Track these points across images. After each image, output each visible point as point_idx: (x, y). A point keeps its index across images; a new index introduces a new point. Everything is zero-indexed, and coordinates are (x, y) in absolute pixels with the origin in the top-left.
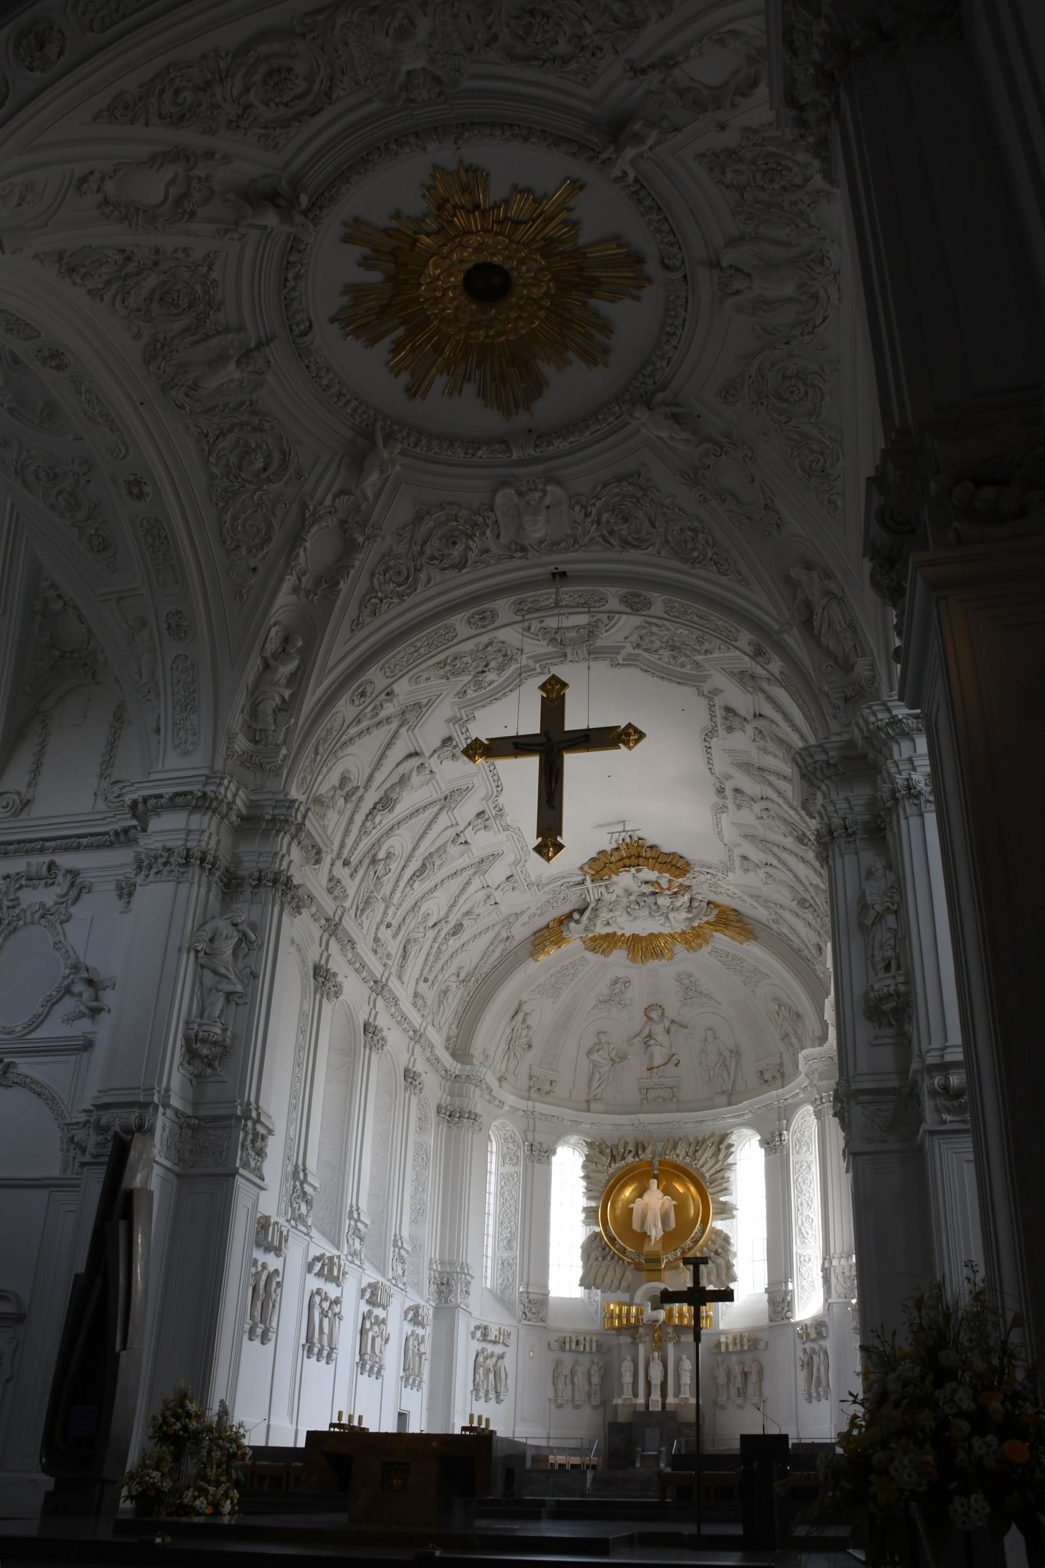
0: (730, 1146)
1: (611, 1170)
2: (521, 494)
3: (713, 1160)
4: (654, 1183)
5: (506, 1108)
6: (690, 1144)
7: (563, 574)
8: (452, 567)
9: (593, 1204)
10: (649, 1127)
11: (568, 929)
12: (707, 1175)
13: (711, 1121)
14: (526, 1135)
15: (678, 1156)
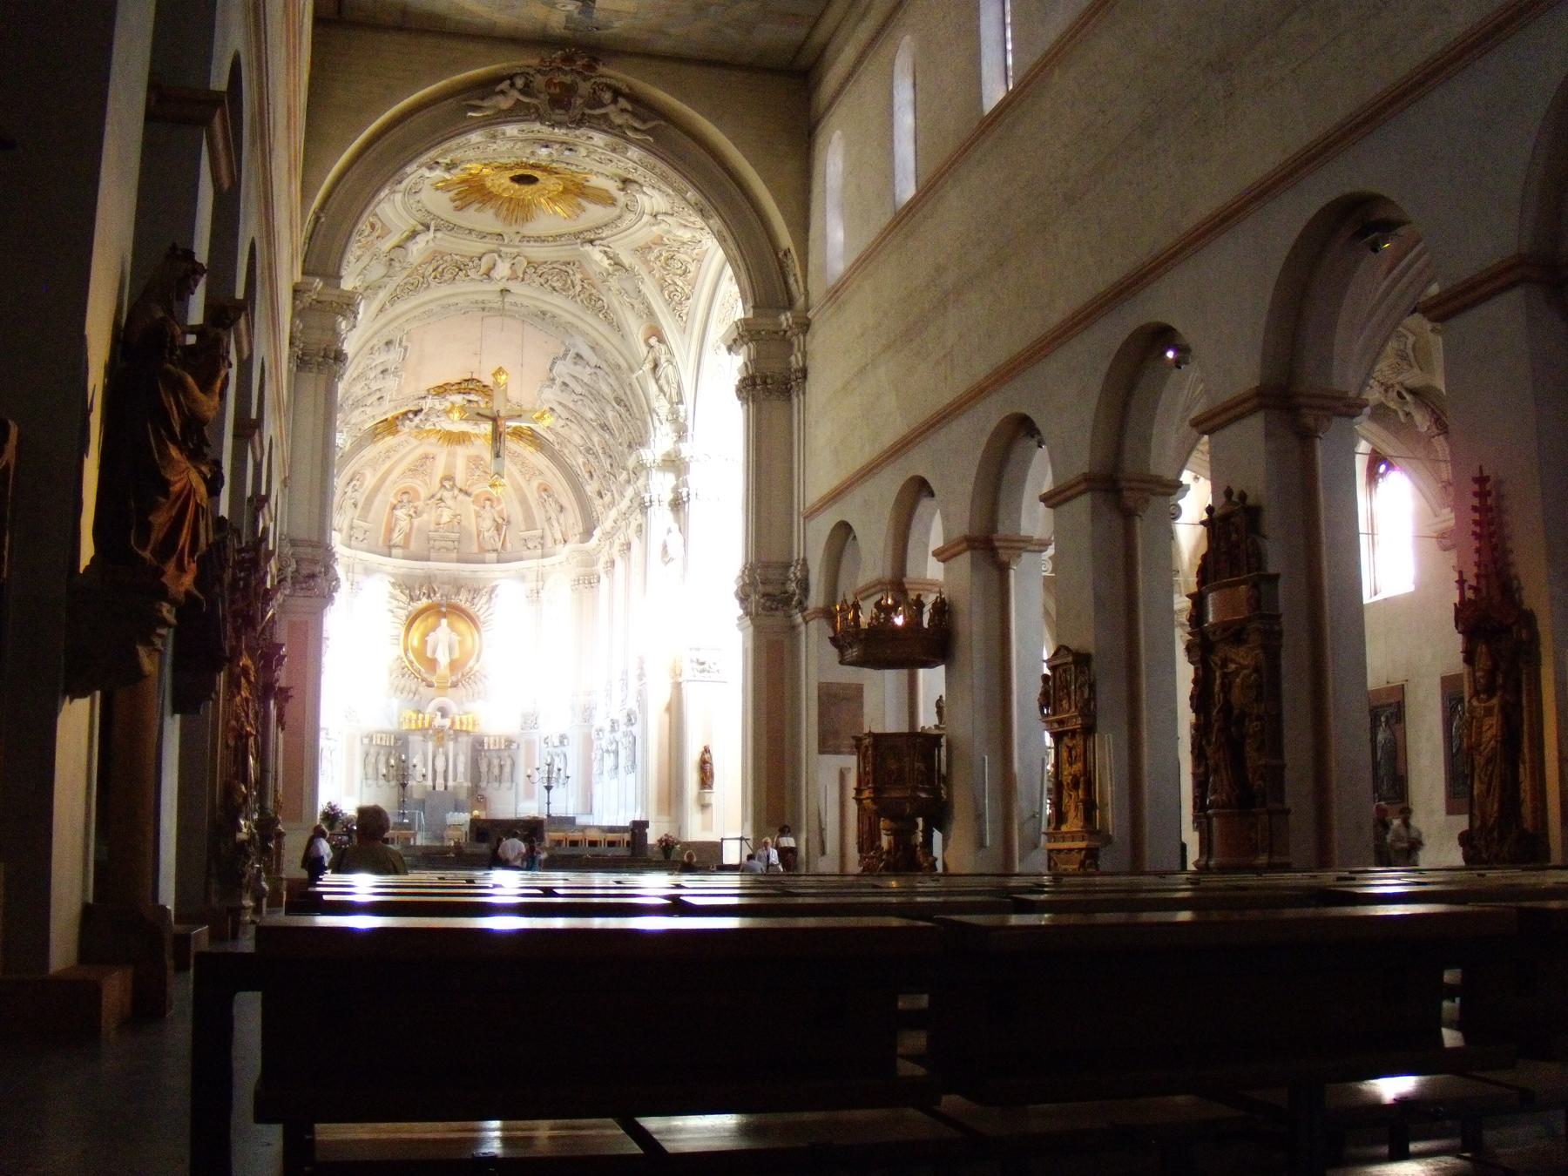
0: (497, 596)
1: (410, 608)
3: (486, 607)
6: (469, 591)
9: (395, 632)
10: (436, 572)
11: (403, 425)
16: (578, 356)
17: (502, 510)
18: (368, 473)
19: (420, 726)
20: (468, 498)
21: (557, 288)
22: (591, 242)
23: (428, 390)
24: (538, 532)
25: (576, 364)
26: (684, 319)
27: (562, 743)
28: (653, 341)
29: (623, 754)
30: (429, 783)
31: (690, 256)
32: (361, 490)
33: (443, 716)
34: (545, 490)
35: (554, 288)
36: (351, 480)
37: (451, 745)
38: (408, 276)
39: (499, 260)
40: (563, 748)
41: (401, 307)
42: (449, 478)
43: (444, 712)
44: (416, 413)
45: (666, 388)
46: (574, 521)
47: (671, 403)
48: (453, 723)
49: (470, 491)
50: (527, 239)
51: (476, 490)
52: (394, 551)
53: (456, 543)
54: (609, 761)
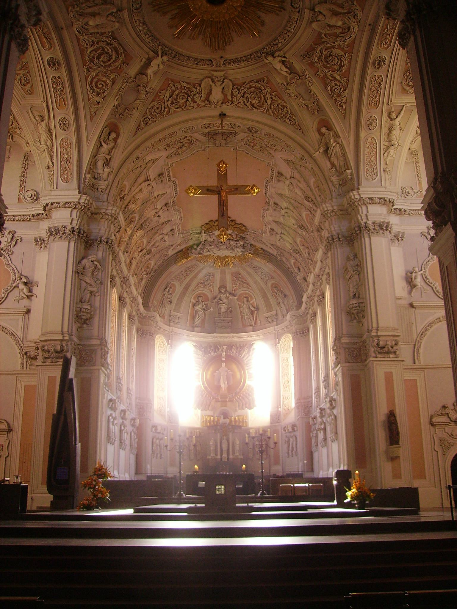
0: (254, 349)
2: (213, 82)
4: (223, 365)
5: (162, 330)
7: (225, 115)
8: (180, 107)
10: (219, 339)
12: (245, 361)
13: (244, 337)
14: (169, 342)
15: (233, 353)
16: (279, 173)
17: (254, 303)
18: (177, 284)
19: (212, 423)
20: (234, 297)
21: (255, 105)
22: (273, 55)
23: (201, 227)
24: (274, 312)
25: (279, 181)
26: (344, 107)
27: (293, 429)
28: (324, 130)
29: (328, 428)
30: (219, 457)
31: (343, 49)
32: (174, 295)
33: (224, 418)
34: (275, 287)
35: (253, 105)
36: (166, 288)
37: (230, 434)
38: (153, 101)
39: (213, 85)
40: (294, 433)
41: (153, 129)
42: (223, 286)
43: (226, 415)
44: (198, 245)
45: (336, 163)
46: (292, 301)
47: (340, 173)
48: (231, 421)
49: (235, 293)
50: (227, 62)
51: (239, 292)
52: (196, 329)
53: (230, 323)
54: (321, 435)
